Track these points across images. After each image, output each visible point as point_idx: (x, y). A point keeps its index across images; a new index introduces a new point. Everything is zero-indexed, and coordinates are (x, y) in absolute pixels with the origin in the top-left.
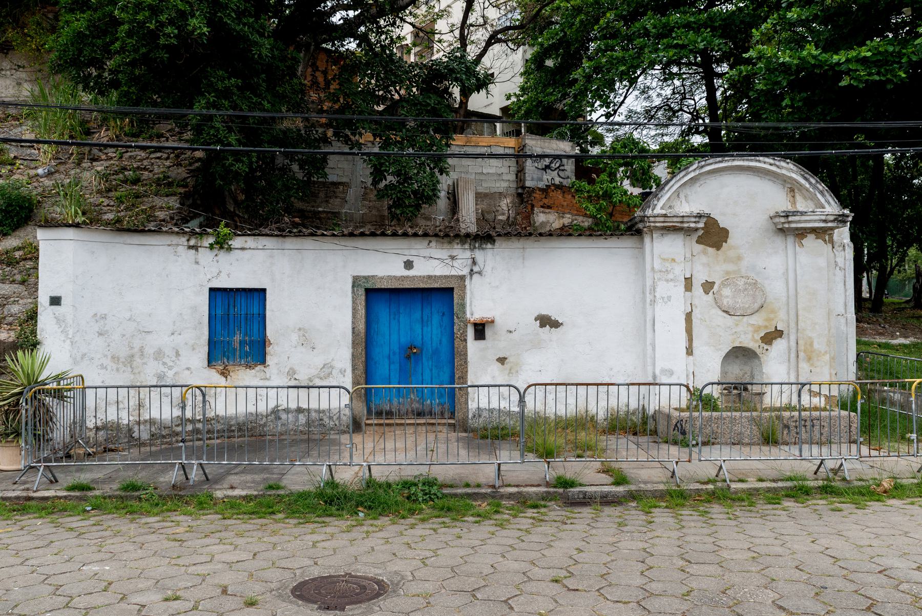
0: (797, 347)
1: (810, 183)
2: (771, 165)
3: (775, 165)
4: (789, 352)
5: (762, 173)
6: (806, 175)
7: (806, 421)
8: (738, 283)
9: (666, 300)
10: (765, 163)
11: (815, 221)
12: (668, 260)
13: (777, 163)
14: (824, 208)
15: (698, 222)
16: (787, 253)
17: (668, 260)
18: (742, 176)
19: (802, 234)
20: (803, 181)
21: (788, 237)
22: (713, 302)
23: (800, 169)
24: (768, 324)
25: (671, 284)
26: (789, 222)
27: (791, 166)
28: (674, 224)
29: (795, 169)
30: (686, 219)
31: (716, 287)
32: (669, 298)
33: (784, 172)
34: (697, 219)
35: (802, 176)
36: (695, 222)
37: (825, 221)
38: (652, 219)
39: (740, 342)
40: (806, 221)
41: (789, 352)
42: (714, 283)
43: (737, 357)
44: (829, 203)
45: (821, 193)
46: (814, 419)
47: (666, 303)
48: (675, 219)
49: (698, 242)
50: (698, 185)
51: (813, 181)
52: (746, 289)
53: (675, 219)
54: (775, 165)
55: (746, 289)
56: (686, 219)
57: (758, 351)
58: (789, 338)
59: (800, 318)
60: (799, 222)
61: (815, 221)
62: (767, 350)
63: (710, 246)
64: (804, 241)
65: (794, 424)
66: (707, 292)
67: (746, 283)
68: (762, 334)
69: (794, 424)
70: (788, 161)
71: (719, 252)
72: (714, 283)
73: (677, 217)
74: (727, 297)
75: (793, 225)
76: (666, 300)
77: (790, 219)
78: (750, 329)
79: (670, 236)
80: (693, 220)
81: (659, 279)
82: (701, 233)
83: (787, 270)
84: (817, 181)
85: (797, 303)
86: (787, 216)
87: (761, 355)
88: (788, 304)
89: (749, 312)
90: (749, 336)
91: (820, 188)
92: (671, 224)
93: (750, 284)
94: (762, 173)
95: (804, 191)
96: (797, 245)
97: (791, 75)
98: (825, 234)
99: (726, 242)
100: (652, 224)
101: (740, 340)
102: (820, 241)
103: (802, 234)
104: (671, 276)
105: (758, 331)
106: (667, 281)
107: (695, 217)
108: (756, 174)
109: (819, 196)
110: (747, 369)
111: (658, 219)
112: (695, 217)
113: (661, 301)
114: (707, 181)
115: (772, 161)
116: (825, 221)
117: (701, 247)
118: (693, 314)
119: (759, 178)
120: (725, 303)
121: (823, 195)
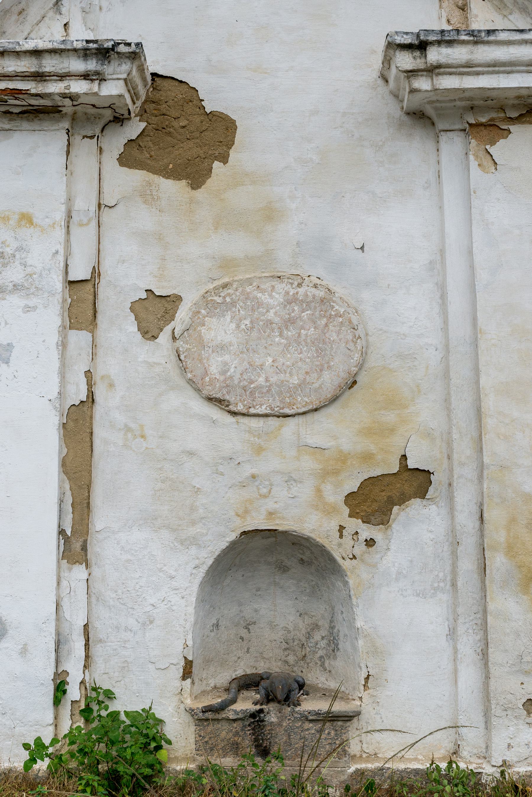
0: (481, 530)
4: (454, 555)
8: (264, 298)
16: (440, 195)
19: (491, 125)
21: (444, 137)
24: (373, 448)
28: (11, 85)
34: (92, 65)
36: (86, 76)
39: (271, 514)
41: (454, 555)
42: (179, 298)
43: (283, 569)
52: (290, 321)
55: (290, 321)
58: (451, 499)
59: (490, 422)
62: (370, 543)
67: (291, 301)
68: (353, 485)
71: (200, 194)
72: (179, 298)
73: (17, 54)
74: (222, 348)
79: (17, 135)
83: (442, 252)
85: (477, 371)
87: (346, 564)
88: (446, 375)
96: (473, 163)
101: (270, 505)
105: (336, 472)
118: (99, 410)
120: (214, 369)
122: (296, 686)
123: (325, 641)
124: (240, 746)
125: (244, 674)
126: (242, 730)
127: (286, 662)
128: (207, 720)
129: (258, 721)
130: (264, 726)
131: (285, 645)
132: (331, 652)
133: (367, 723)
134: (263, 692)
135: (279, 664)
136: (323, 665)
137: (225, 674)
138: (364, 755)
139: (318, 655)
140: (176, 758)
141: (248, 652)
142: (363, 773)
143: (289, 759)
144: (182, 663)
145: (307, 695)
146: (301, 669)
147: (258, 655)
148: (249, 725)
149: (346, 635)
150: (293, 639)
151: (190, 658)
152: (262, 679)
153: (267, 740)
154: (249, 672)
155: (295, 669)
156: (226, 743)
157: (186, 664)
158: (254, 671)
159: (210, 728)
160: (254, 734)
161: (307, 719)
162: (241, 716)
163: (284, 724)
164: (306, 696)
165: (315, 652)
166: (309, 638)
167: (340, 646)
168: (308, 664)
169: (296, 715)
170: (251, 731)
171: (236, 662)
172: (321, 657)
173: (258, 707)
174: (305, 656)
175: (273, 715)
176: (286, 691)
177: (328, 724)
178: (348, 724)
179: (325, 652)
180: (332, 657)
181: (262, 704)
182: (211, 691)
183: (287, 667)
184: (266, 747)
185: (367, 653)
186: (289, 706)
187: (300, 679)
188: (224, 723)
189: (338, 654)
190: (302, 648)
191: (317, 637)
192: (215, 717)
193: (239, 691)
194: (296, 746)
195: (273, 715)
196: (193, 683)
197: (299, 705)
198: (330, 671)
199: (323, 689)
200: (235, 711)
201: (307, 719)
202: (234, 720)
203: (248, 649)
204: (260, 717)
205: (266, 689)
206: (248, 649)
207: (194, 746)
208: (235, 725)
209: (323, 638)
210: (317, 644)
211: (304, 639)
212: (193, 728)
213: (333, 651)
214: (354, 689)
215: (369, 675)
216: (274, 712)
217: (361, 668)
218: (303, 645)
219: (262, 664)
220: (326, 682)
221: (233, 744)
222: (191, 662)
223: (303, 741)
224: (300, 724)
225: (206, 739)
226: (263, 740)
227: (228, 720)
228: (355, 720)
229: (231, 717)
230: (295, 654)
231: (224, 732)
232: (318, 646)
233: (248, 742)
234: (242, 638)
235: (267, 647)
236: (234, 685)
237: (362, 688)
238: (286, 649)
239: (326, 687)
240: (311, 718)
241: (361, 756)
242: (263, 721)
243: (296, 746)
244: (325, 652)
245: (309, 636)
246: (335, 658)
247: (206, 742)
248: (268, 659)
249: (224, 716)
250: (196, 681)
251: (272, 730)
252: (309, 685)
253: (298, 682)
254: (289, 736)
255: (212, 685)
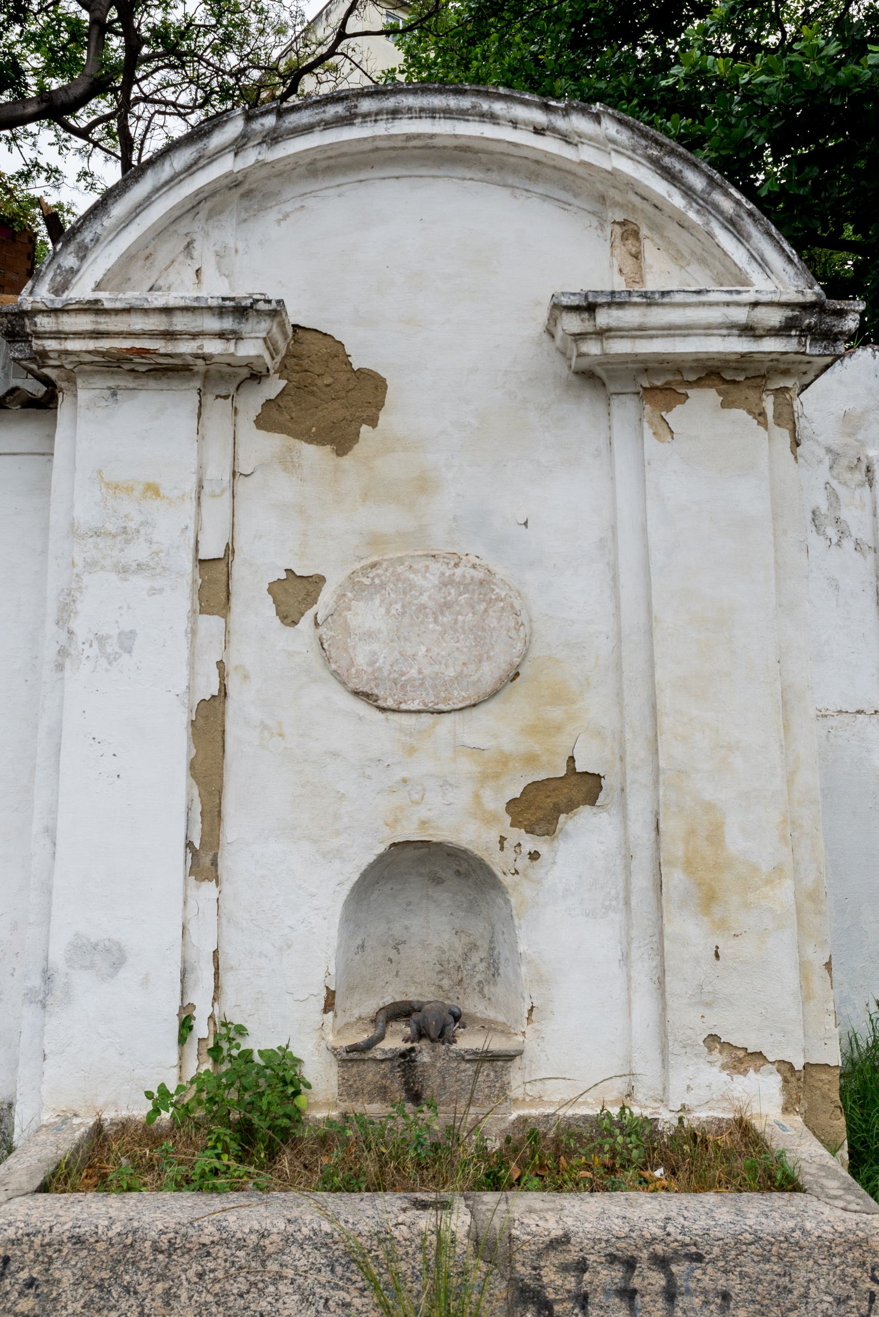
0: (657, 842)
1: (688, 192)
2: (539, 131)
3: (553, 130)
4: (627, 868)
5: (515, 171)
6: (667, 161)
7: (630, 1264)
8: (417, 579)
9: (112, 647)
10: (514, 124)
11: (708, 330)
12: (130, 490)
13: (560, 123)
14: (745, 281)
15: (236, 336)
17: (130, 490)
18: (441, 183)
20: (659, 186)
22: (313, 656)
23: (644, 135)
24: (537, 748)
25: (140, 582)
26: (602, 334)
27: (610, 128)
28: (138, 344)
29: (624, 136)
30: (180, 323)
31: (326, 597)
32: (127, 641)
33: (587, 154)
34: (228, 323)
35: (656, 163)
36: (221, 335)
37: (748, 330)
38: (44, 323)
39: (423, 823)
40: (671, 330)
41: (627, 868)
43: (437, 881)
44: (763, 264)
45: (732, 225)
46: (676, 1257)
47: (112, 659)
48: (138, 323)
49: (262, 423)
50: (273, 215)
51: (697, 182)
52: (447, 606)
53: (138, 323)
54: (553, 130)
55: (447, 606)
56: (180, 323)
57: (497, 862)
58: (624, 806)
59: (666, 722)
60: (641, 332)
61: (708, 330)
62: (534, 856)
63: (312, 439)
64: (675, 416)
65: (570, 1283)
66: (289, 618)
67: (447, 583)
68: (516, 791)
69: (570, 1283)
70: (598, 107)
71: (346, 461)
73: (146, 311)
74: (370, 636)
75: (619, 347)
76: (112, 647)
77: (604, 318)
78: (466, 766)
80: (213, 324)
81: (92, 565)
82: (274, 386)
83: (614, 528)
84: (711, 180)
85: (651, 663)
86: (590, 308)
87: (507, 880)
88: (618, 666)
89: (459, 696)
90: (462, 797)
91: (727, 205)
92: (127, 344)
93: (464, 585)
94: (515, 170)
95: (672, 230)
96: (648, 432)
97: (772, 119)
98: (762, 390)
99: (373, 422)
100: (51, 345)
101: (423, 812)
102: (740, 414)
103: (667, 389)
104: (138, 552)
105: (497, 776)
106: (123, 570)
107: (220, 311)
108: (494, 176)
109: (725, 239)
110: (478, 928)
111: (70, 323)
112: (220, 311)
113: (95, 650)
114: (310, 202)
115: (539, 117)
116: (748, 330)
117: (275, 441)
118: (232, 706)
119: (506, 193)
120: (361, 659)
121: (740, 236)
122: (451, 1019)
123: (484, 964)
124: (389, 1090)
125: (392, 1001)
126: (391, 1071)
127: (440, 987)
128: (351, 1060)
129: (408, 1061)
130: (416, 1067)
131: (438, 968)
132: (491, 976)
133: (531, 1061)
134: (414, 1026)
135: (433, 988)
136: (481, 991)
137: (372, 1002)
138: (528, 1099)
139: (476, 980)
140: (316, 1103)
141: (397, 975)
142: (526, 1120)
143: (443, 1105)
144: (324, 993)
145: (464, 1027)
146: (457, 995)
147: (408, 979)
148: (399, 1066)
149: (507, 959)
150: (448, 960)
151: (332, 988)
152: (414, 1010)
153: (418, 1083)
154: (398, 999)
155: (451, 995)
156: (372, 1086)
157: (328, 994)
158: (404, 998)
159: (355, 1070)
160: (404, 1076)
161: (463, 1059)
162: (389, 1055)
163: (438, 1065)
164: (462, 1030)
165: (473, 976)
166: (465, 960)
167: (501, 971)
168: (465, 989)
169: (451, 1054)
170: (401, 1073)
171: (383, 987)
172: (480, 982)
173: (409, 1045)
174: (461, 980)
175: (425, 1054)
176: (440, 1027)
177: (487, 1064)
178: (509, 1064)
179: (484, 976)
180: (491, 982)
181: (413, 1042)
182: (356, 1023)
183: (441, 993)
184: (417, 1091)
185: (531, 981)
186: (443, 1043)
187: (456, 1010)
188: (370, 1064)
189: (499, 979)
190: (458, 970)
191: (475, 958)
192: (360, 1057)
193: (387, 1022)
194: (452, 1090)
195: (425, 1054)
196: (335, 1016)
197: (455, 1042)
198: (489, 999)
199: (481, 1019)
200: (383, 1051)
201: (463, 1059)
202: (382, 1061)
203: (397, 972)
204: (411, 1057)
205: (418, 1023)
206: (397, 972)
207: (337, 1090)
208: (383, 1066)
209: (482, 960)
210: (475, 967)
211: (460, 961)
212: (335, 1069)
213: (493, 975)
214: (516, 1021)
215: (532, 1007)
216: (427, 1050)
217: (524, 999)
218: (459, 967)
219: (413, 989)
220: (485, 1011)
221: (381, 1088)
222: (334, 992)
223: (459, 1083)
224: (456, 1064)
225: (350, 1083)
226: (414, 1083)
227: (375, 1060)
228: (518, 1058)
229: (378, 1057)
230: (450, 978)
231: (371, 1074)
232: (477, 969)
233: (397, 1085)
234: (390, 960)
235: (419, 970)
236: (381, 1018)
237: (525, 1021)
238: (440, 972)
239: (485, 1016)
240: (468, 1057)
241: (524, 1100)
242: (414, 1061)
243: (452, 1090)
244: (484, 976)
245: (466, 957)
246: (495, 984)
247: (351, 1086)
248: (419, 983)
249: (371, 1056)
250: (339, 1013)
251: (424, 1071)
252: (466, 1015)
253: (452, 1013)
254: (444, 1078)
255: (357, 1015)
